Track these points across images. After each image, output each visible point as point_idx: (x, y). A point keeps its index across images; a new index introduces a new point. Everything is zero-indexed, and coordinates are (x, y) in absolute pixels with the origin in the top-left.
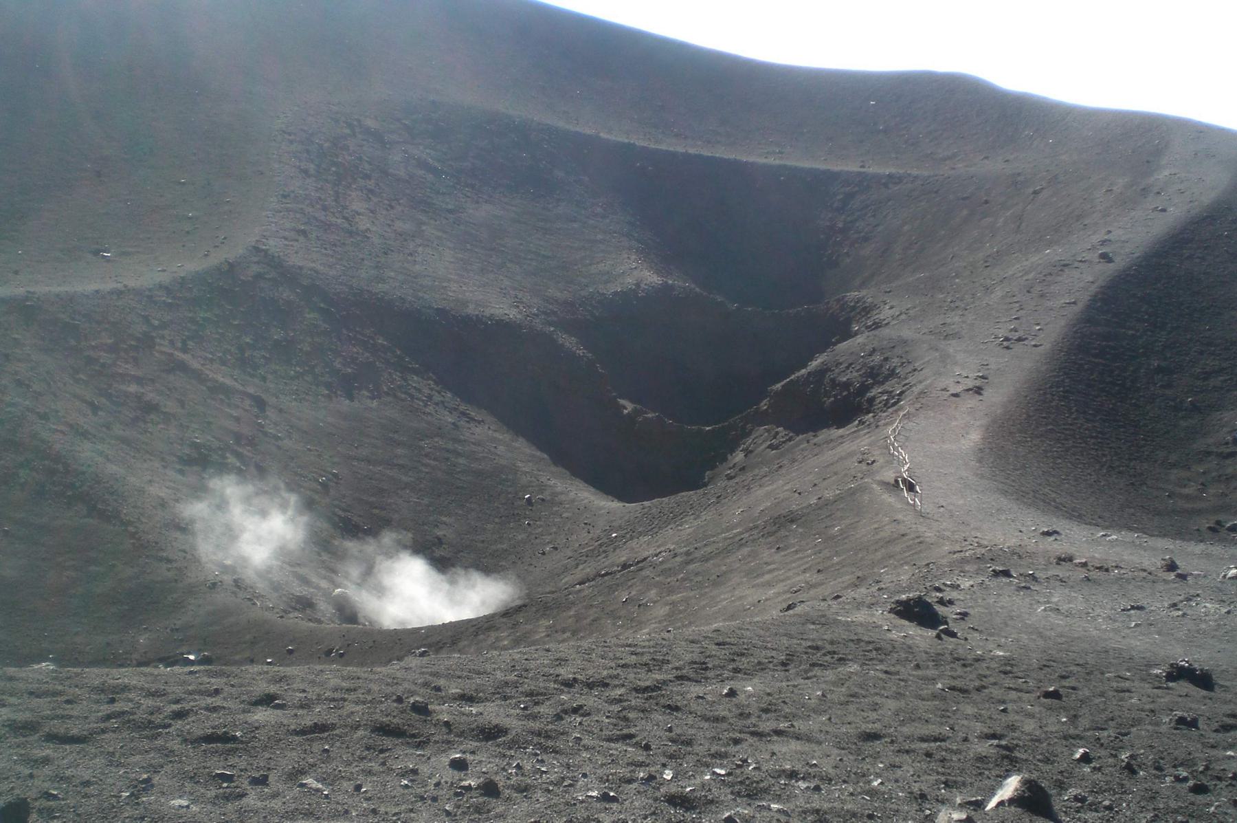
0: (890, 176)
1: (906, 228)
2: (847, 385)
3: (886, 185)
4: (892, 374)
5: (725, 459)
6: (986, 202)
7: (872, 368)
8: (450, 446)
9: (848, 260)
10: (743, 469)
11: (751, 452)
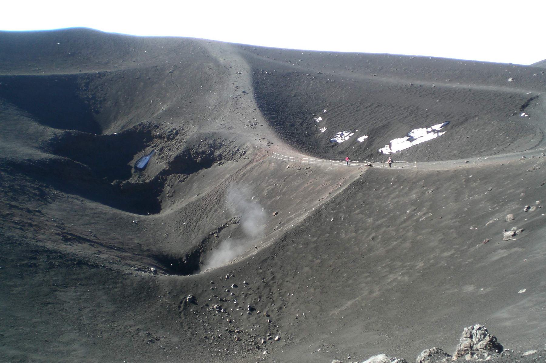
0: (99, 74)
1: (120, 93)
2: (203, 152)
3: (99, 77)
4: (221, 145)
5: (163, 191)
6: (149, 79)
7: (211, 145)
8: (93, 212)
9: (102, 110)
10: (174, 192)
11: (172, 185)
